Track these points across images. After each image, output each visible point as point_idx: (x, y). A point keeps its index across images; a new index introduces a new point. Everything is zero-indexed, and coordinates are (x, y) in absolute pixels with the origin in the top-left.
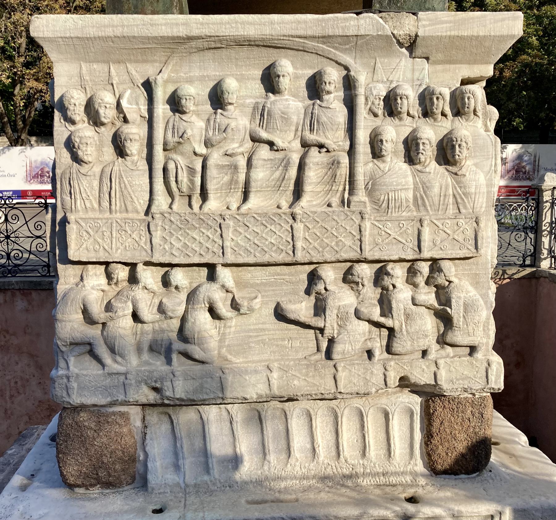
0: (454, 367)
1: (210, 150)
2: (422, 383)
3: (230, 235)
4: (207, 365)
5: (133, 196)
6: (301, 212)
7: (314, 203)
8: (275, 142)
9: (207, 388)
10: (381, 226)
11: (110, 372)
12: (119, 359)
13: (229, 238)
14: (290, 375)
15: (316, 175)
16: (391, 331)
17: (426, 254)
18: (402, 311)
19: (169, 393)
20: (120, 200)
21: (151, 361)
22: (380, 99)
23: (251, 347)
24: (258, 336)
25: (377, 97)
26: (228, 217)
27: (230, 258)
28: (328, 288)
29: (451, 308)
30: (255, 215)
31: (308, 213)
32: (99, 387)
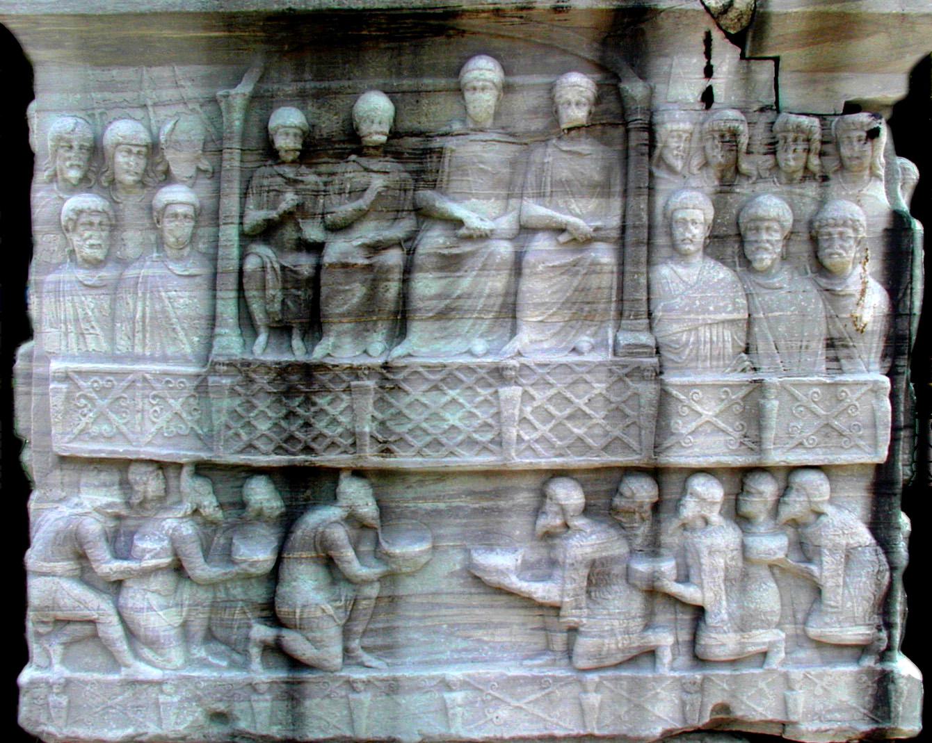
0: (822, 687)
1: (331, 236)
2: (758, 718)
3: (371, 408)
4: (321, 674)
5: (178, 328)
6: (518, 365)
7: (546, 345)
8: (465, 220)
9: (320, 718)
10: (682, 397)
11: (131, 678)
12: (147, 653)
13: (369, 417)
14: (489, 697)
15: (550, 286)
16: (699, 613)
17: (777, 456)
18: (722, 574)
19: (243, 725)
20: (152, 336)
21: (210, 658)
22: (680, 137)
23: (411, 639)
24: (425, 617)
25: (675, 134)
26: (366, 372)
27: (371, 458)
28: (570, 524)
29: (821, 568)
30: (421, 369)
31: (534, 367)
32: (111, 707)
